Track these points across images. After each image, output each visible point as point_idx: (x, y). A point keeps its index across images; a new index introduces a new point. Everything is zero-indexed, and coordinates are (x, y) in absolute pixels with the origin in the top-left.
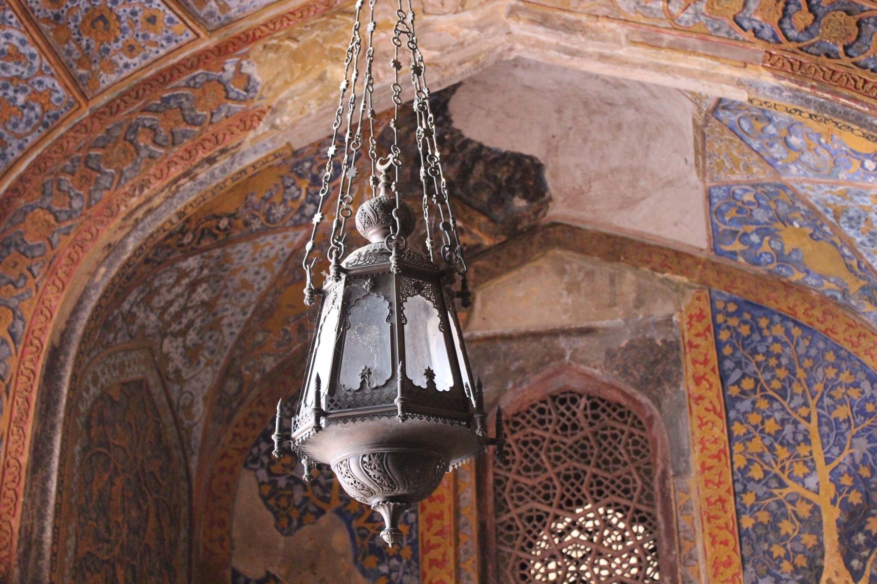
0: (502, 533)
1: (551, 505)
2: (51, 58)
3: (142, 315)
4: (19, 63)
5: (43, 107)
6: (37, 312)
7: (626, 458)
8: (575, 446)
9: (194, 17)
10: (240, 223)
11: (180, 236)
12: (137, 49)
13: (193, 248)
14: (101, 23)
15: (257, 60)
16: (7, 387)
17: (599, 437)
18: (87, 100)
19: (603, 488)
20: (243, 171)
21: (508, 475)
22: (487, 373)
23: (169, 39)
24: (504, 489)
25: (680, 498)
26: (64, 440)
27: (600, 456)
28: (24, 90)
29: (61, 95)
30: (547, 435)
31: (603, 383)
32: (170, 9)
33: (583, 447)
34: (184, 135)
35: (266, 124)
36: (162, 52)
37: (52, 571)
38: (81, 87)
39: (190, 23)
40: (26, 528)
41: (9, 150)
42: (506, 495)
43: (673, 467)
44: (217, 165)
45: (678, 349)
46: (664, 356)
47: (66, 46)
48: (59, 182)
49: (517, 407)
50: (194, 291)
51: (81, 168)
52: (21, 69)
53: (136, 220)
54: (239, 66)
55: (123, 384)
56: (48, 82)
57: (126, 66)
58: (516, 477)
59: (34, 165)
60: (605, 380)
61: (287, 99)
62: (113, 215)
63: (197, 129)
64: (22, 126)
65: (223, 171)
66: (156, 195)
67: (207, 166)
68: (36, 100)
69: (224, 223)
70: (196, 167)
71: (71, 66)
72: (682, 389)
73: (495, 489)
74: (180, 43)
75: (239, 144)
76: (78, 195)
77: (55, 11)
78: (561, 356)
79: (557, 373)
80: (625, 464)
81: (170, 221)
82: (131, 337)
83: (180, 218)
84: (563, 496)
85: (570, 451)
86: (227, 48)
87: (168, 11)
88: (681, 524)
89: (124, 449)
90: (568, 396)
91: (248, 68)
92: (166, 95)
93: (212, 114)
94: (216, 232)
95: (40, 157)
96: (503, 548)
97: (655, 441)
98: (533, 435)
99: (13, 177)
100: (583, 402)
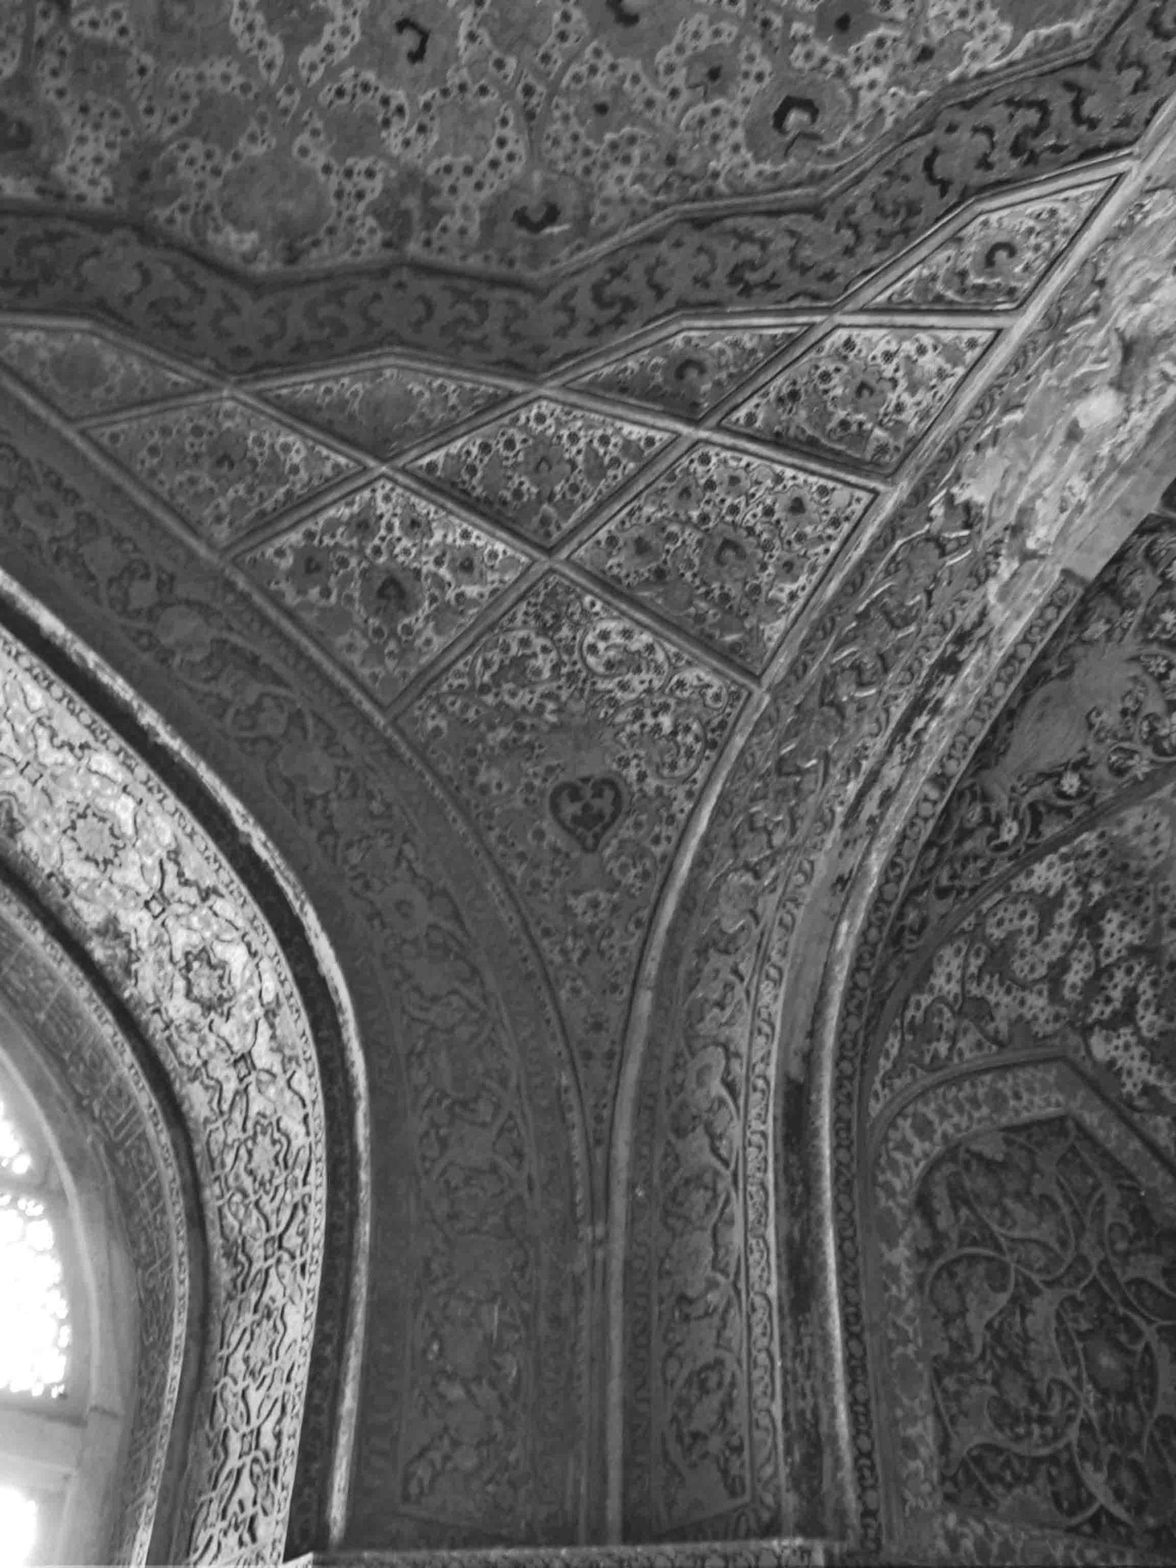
2: (674, 637)
3: (1006, 1000)
4: (638, 670)
5: (698, 718)
6: (755, 1031)
9: (855, 466)
10: (1102, 772)
11: (989, 830)
12: (798, 563)
13: (1029, 847)
14: (729, 554)
15: (973, 475)
16: (735, 1175)
18: (757, 679)
20: (1011, 659)
23: (835, 523)
26: (841, 1240)
28: (665, 707)
29: (715, 689)
32: (813, 473)
34: (898, 649)
35: (1011, 556)
36: (834, 547)
37: (863, 1488)
38: (738, 659)
39: (852, 479)
40: (801, 1414)
41: (676, 806)
44: (968, 670)
47: (692, 610)
48: (751, 819)
50: (1099, 932)
51: (776, 782)
52: (645, 676)
53: (871, 820)
54: (950, 500)
55: (1008, 1129)
56: (690, 676)
57: (793, 596)
59: (718, 811)
61: (1032, 499)
62: (828, 826)
63: (912, 629)
64: (681, 762)
65: (979, 673)
66: (882, 763)
67: (949, 678)
68: (687, 714)
69: (1070, 783)
70: (928, 686)
71: (711, 637)
74: (855, 518)
75: (983, 614)
76: (778, 824)
77: (654, 565)
81: (926, 799)
82: (1001, 1045)
83: (943, 788)
86: (926, 485)
87: (812, 479)
89: (1045, 1247)
91: (962, 495)
92: (861, 608)
93: (929, 594)
94: (1062, 803)
95: (721, 797)
99: (693, 843)
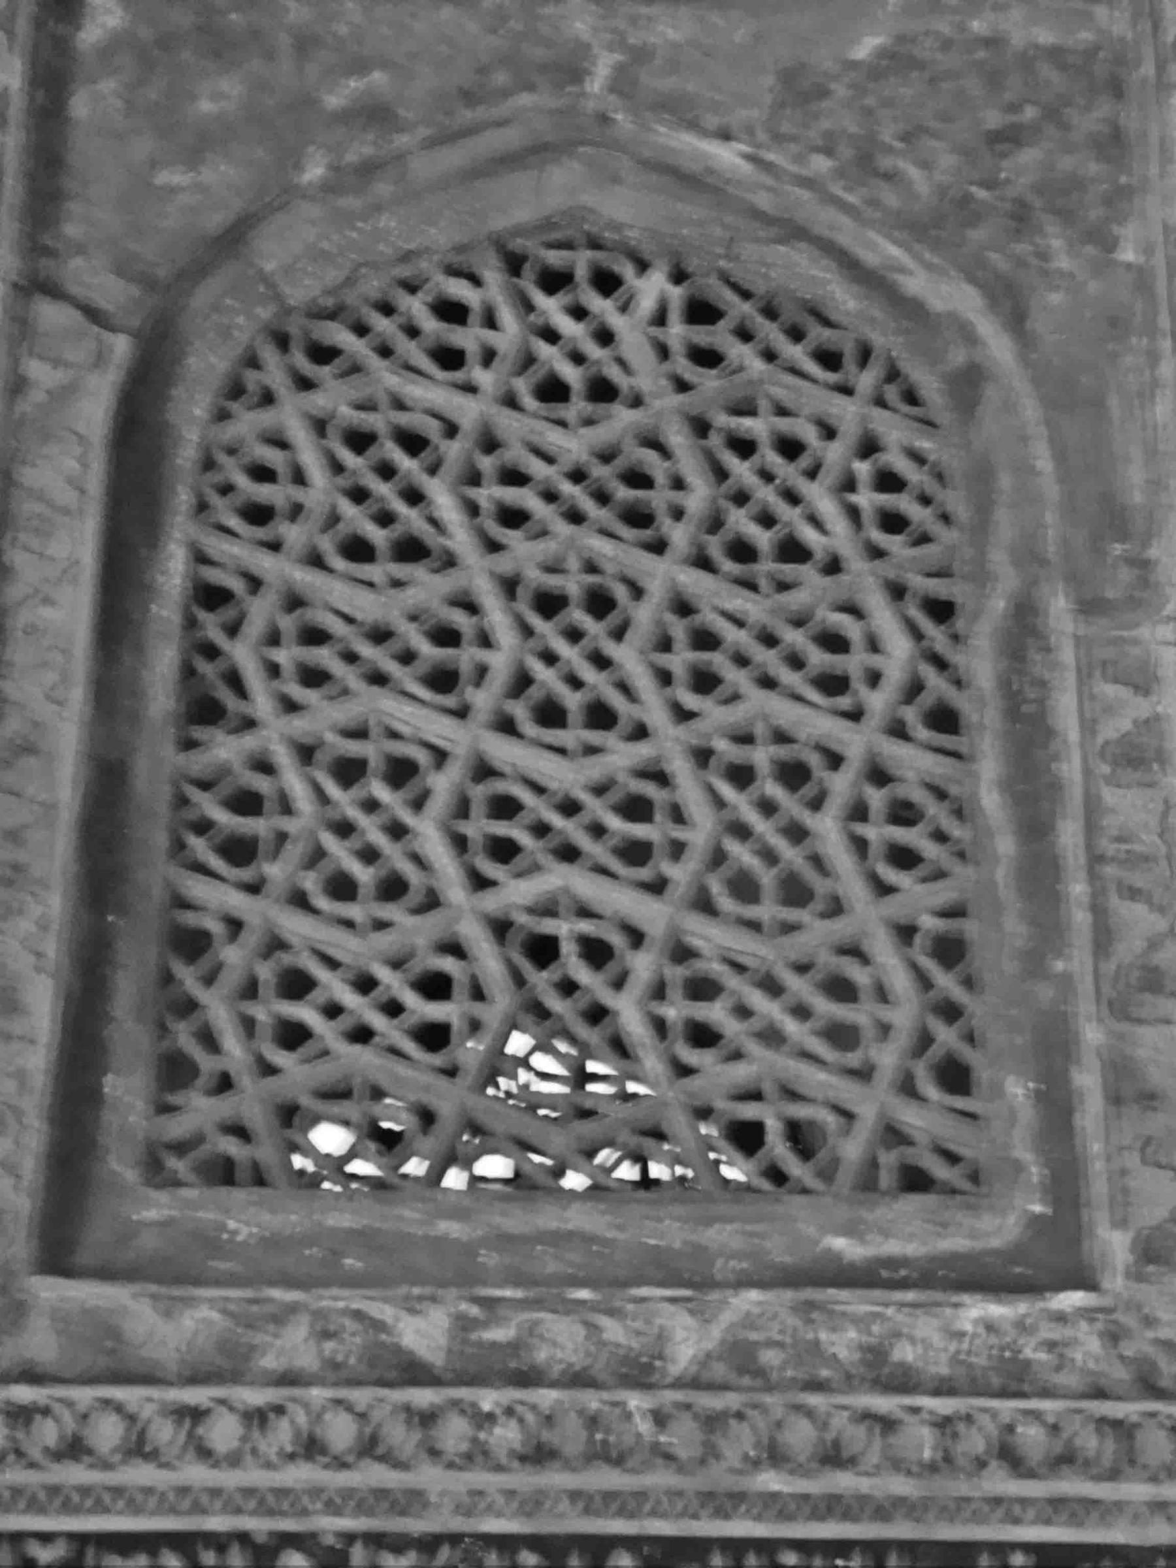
0: (203, 827)
1: (462, 713)
7: (839, 536)
8: (599, 471)
17: (715, 440)
19: (718, 661)
21: (265, 563)
22: (206, 106)
24: (233, 630)
25: (1110, 710)
27: (715, 524)
30: (469, 412)
31: (756, 214)
33: (638, 479)
42: (243, 654)
43: (1073, 579)
45: (1117, 89)
46: (1053, 114)
49: (334, 275)
58: (304, 577)
60: (763, 201)
72: (1128, 254)
73: (191, 623)
78: (570, 70)
79: (537, 153)
80: (833, 566)
84: (522, 682)
85: (567, 488)
88: (1111, 823)
90: (582, 262)
96: (198, 888)
97: (982, 477)
98: (400, 405)
100: (651, 288)
